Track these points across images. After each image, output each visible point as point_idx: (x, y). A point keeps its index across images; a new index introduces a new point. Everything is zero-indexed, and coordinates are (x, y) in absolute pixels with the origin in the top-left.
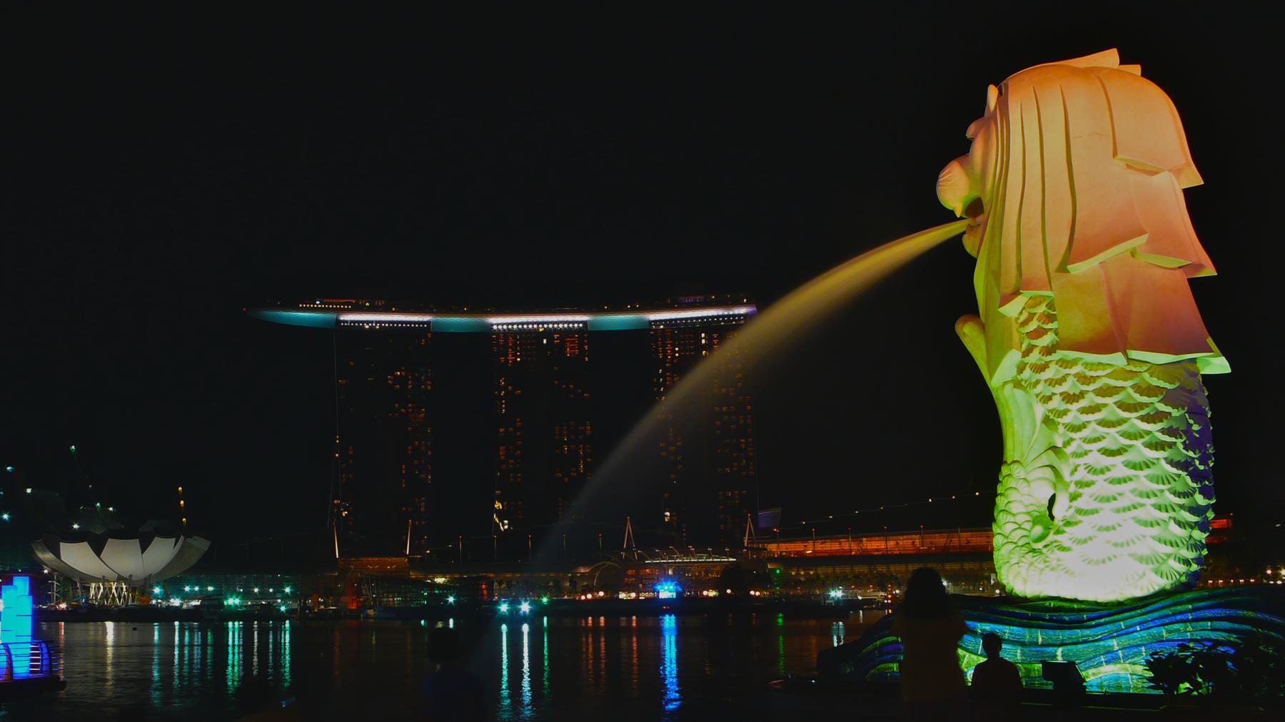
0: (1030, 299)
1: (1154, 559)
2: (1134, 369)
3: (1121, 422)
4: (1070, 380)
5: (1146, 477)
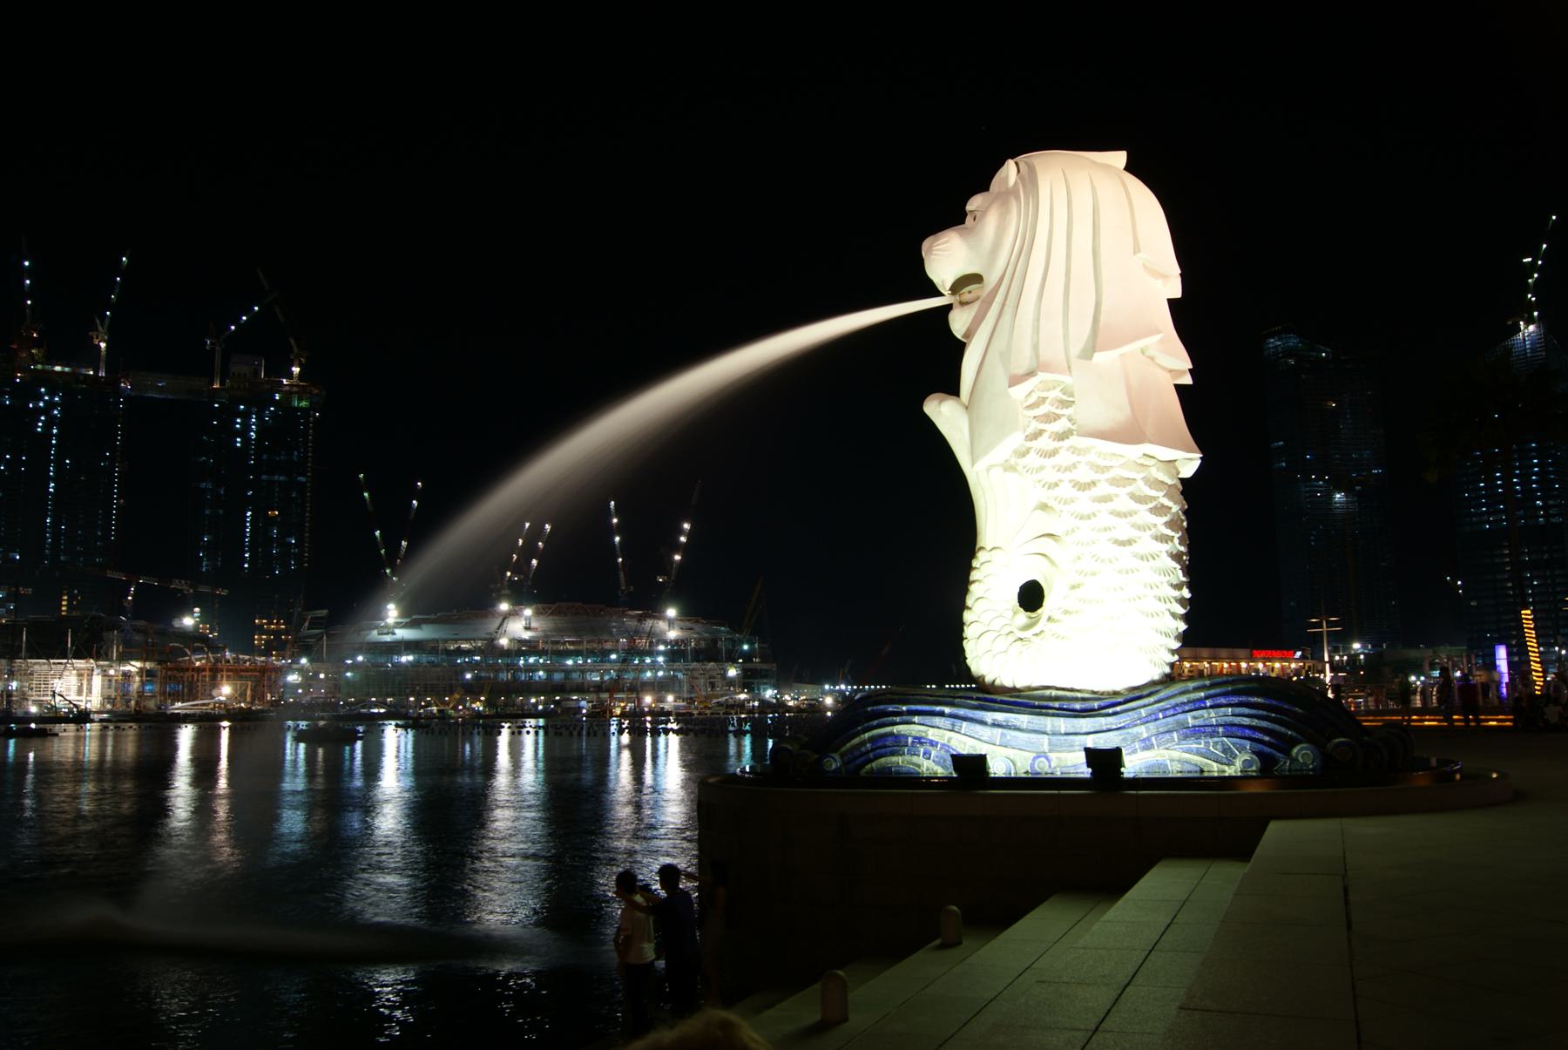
0: (1040, 383)
2: (1145, 463)
3: (1131, 514)
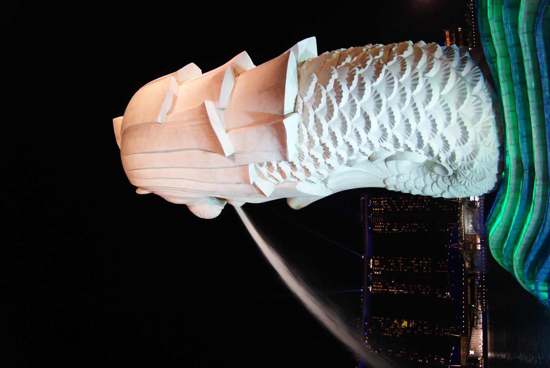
0: (260, 176)
1: (463, 88)
2: (301, 108)
4: (312, 152)
5: (387, 97)
